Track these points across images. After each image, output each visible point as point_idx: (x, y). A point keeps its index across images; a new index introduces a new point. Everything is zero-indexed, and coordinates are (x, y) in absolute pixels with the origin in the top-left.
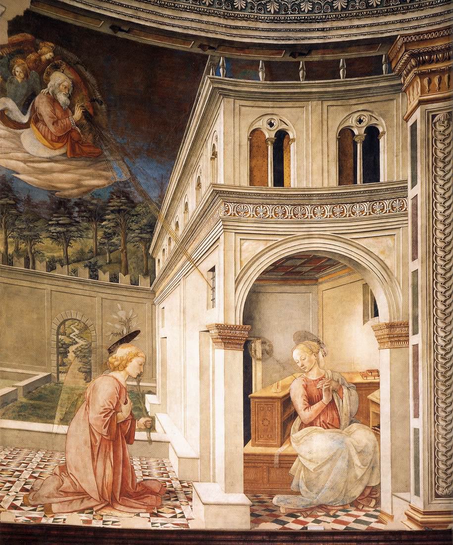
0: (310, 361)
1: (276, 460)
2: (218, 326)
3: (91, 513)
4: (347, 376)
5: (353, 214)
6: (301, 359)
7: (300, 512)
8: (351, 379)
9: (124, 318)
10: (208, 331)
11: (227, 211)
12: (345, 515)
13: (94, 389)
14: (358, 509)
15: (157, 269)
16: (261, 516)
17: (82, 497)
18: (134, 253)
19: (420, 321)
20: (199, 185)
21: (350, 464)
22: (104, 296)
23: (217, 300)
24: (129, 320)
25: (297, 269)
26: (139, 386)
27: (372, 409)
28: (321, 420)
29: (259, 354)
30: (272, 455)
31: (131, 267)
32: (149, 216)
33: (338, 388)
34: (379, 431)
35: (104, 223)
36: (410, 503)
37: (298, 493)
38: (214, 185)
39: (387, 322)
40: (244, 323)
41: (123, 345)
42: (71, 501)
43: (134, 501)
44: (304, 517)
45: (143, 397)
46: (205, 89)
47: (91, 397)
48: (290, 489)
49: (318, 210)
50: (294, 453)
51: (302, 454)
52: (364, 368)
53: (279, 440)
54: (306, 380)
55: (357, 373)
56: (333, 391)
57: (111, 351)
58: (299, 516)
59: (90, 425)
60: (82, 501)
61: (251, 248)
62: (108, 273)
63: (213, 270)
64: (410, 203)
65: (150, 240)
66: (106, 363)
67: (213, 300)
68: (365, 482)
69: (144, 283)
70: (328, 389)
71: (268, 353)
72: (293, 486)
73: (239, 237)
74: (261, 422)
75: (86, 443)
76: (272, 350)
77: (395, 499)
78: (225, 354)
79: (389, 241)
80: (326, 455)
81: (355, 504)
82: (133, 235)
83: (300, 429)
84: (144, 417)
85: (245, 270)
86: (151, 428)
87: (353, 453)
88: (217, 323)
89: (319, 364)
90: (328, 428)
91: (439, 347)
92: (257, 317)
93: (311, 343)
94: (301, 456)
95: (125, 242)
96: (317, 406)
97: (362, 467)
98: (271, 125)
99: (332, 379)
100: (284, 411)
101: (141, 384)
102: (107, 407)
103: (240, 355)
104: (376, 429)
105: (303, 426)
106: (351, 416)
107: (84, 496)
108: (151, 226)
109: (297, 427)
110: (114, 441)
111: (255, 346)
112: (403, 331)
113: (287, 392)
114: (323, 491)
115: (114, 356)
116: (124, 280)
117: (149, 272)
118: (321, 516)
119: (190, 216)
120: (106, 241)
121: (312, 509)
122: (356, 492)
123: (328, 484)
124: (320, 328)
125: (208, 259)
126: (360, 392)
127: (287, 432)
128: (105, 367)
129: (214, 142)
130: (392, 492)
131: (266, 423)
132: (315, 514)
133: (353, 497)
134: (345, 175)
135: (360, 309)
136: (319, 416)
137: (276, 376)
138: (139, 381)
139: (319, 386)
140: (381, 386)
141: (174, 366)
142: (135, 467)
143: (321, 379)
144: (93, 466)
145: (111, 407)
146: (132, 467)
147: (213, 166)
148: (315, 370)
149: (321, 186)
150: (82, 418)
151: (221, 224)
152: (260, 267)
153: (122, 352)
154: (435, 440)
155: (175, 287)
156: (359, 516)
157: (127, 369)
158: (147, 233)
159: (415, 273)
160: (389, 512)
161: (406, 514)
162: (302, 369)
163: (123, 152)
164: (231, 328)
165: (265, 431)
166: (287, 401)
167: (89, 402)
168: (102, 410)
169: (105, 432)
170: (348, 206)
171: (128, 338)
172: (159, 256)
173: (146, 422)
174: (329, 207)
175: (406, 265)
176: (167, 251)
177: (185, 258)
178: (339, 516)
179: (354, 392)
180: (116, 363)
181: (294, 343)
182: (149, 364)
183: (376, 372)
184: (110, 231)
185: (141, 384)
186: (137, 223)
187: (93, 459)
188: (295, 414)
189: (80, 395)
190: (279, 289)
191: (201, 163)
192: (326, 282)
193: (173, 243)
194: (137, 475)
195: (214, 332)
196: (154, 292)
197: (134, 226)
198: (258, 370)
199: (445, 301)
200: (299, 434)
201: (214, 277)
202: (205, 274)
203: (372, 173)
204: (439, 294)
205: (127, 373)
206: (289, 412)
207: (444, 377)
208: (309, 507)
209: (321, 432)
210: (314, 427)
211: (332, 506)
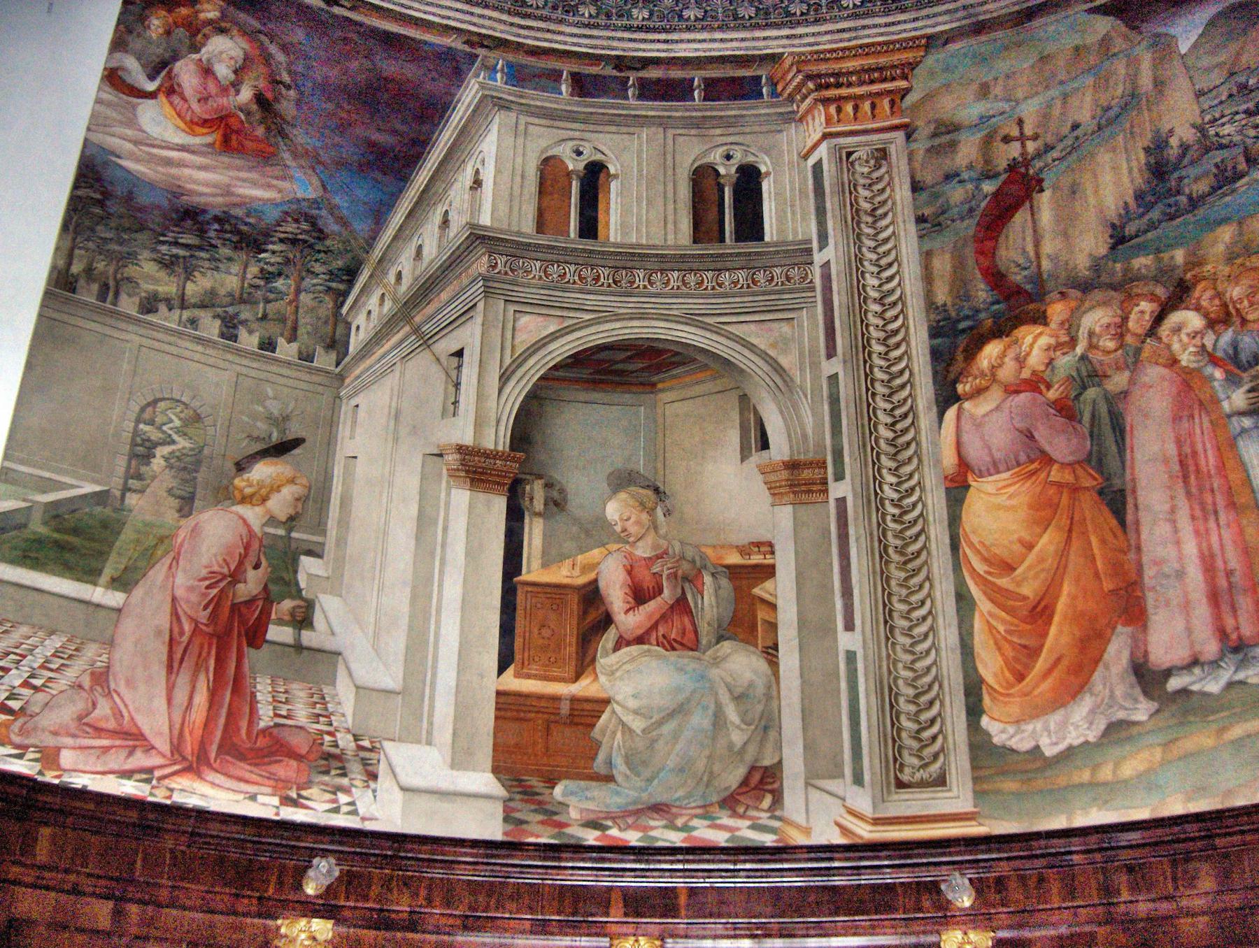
0: (638, 523)
1: (565, 708)
2: (461, 449)
3: (148, 781)
4: (709, 552)
5: (720, 285)
6: (621, 520)
7: (613, 819)
8: (720, 558)
9: (276, 412)
10: (441, 455)
11: (495, 267)
12: (709, 827)
13: (195, 531)
14: (735, 814)
15: (352, 340)
16: (527, 822)
17: (131, 743)
18: (313, 309)
19: (847, 459)
20: (445, 222)
21: (719, 720)
22: (245, 371)
23: (462, 406)
24: (286, 418)
25: (620, 366)
26: (290, 538)
27: (762, 614)
28: (660, 634)
29: (539, 505)
30: (555, 699)
31: (301, 331)
32: (349, 255)
33: (694, 572)
34: (777, 657)
35: (263, 255)
36: (844, 799)
37: (609, 779)
38: (472, 226)
39: (786, 458)
40: (512, 448)
41: (269, 460)
42: (106, 750)
43: (248, 767)
44: (620, 829)
45: (295, 562)
46: (469, 94)
47: (186, 545)
48: (592, 768)
49: (657, 277)
50: (603, 695)
51: (619, 697)
52: (743, 539)
53: (572, 668)
54: (629, 556)
55: (731, 546)
56: (686, 578)
57: (241, 467)
58: (608, 828)
59: (174, 599)
60: (131, 754)
61: (532, 327)
62: (257, 334)
63: (459, 354)
64: (817, 272)
65: (345, 294)
66: (227, 488)
67: (456, 403)
68: (749, 757)
69: (324, 360)
70: (673, 576)
71: (556, 504)
72: (599, 765)
73: (512, 308)
74: (536, 631)
75: (159, 633)
76: (565, 500)
77: (815, 795)
78: (471, 499)
79: (785, 328)
80: (668, 702)
81: (730, 802)
82: (315, 281)
83: (617, 647)
84: (293, 598)
85: (519, 361)
86: (303, 620)
87: (725, 698)
88: (460, 442)
89: (656, 528)
90: (674, 649)
91: (887, 502)
92: (538, 437)
93: (641, 491)
94: (618, 703)
95: (298, 291)
96: (651, 606)
97: (744, 726)
98: (579, 153)
99: (683, 558)
100: (585, 613)
101: (294, 535)
102: (216, 568)
103: (499, 505)
104: (771, 653)
105: (620, 643)
106: (719, 626)
107: (137, 743)
108: (351, 274)
109: (610, 645)
110: (219, 637)
111: (532, 489)
112: (816, 474)
113: (592, 576)
114: (661, 775)
115: (246, 476)
116: (287, 350)
117: (337, 344)
118: (656, 828)
119: (424, 265)
120: (262, 283)
121: (638, 813)
122: (733, 777)
123: (671, 763)
124: (660, 465)
125: (450, 335)
126: (738, 583)
127: (591, 652)
128: (224, 495)
129: (479, 166)
130: (807, 778)
131: (546, 633)
132: (644, 823)
133: (726, 789)
134: (706, 227)
135: (734, 437)
136: (655, 626)
137: (569, 545)
138: (290, 530)
139: (656, 569)
140: (778, 574)
141: (365, 509)
142: (259, 697)
143: (658, 557)
144: (168, 680)
145: (225, 570)
146: (253, 695)
147: (473, 198)
148: (650, 539)
149: (662, 243)
150: (158, 583)
151: (481, 283)
152: (549, 358)
153: (263, 471)
154: (890, 672)
155: (383, 374)
156: (738, 829)
157: (271, 504)
158: (342, 281)
159: (833, 378)
160: (800, 819)
161: (838, 824)
162: (623, 538)
163: (314, 161)
164: (487, 455)
165: (544, 648)
166: (591, 595)
167: (179, 553)
168: (204, 572)
169: (203, 616)
170: (710, 274)
171: (282, 449)
172: (360, 320)
173: (294, 608)
174: (676, 274)
175: (815, 366)
176: (374, 315)
177: (407, 329)
178: (694, 828)
179: (725, 582)
180: (248, 491)
181: (608, 490)
182: (315, 501)
183: (770, 548)
184: (270, 269)
185: (294, 535)
186: (324, 263)
187: (170, 668)
188: (607, 620)
189: (161, 540)
190: (583, 396)
191: (452, 193)
192: (671, 389)
193: (388, 304)
194: (261, 712)
195: (452, 458)
196: (341, 378)
197: (318, 268)
198: (534, 534)
199: (893, 424)
200: (613, 658)
201: (459, 367)
202: (444, 360)
203: (750, 226)
204: (879, 413)
205: (268, 511)
206: (593, 616)
207: (902, 554)
208: (630, 808)
209: (659, 657)
210: (646, 647)
211: (680, 807)
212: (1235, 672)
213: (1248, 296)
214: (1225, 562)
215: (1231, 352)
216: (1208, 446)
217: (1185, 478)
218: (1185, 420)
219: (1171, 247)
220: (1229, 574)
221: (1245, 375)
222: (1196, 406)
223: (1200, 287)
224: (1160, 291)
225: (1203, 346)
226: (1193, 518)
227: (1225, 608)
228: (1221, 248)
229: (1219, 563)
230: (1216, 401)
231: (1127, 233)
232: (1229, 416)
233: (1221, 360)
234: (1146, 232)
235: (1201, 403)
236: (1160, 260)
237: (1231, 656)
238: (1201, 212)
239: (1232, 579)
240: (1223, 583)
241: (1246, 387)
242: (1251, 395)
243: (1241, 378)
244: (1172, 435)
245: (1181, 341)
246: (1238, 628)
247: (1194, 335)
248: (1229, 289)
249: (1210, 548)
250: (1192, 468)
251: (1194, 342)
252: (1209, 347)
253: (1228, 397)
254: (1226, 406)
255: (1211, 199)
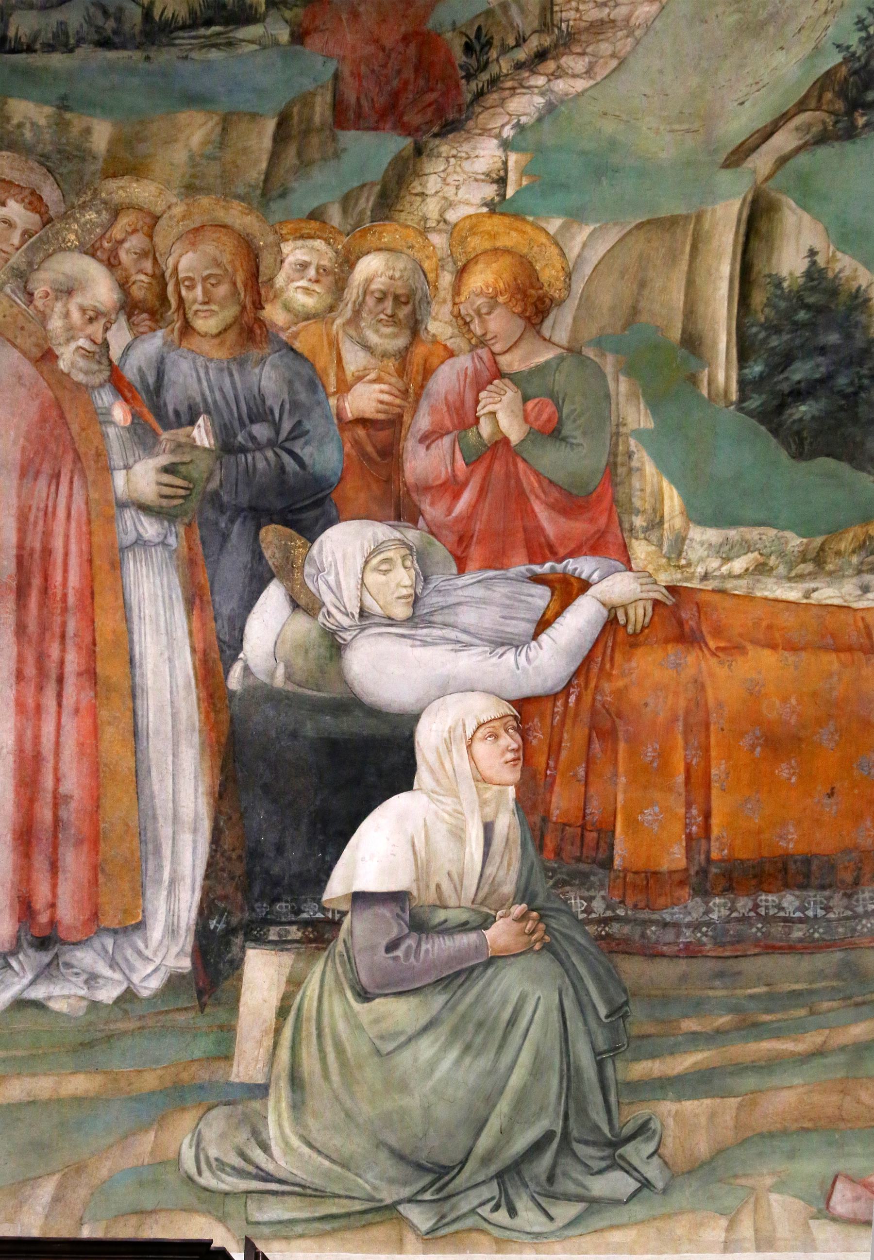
212: (33, 983)
213: (205, 279)
214: (57, 780)
215: (151, 380)
216: (73, 548)
217: (21, 593)
218: (42, 482)
219: (90, 106)
220: (58, 800)
221: (165, 435)
222: (70, 457)
223: (125, 221)
224: (50, 193)
225: (106, 345)
226: (20, 676)
227: (40, 862)
228: (179, 155)
229: (48, 782)
230: (108, 470)
231: (11, 33)
232: (122, 505)
233: (130, 386)
234: (49, 48)
235: (77, 458)
236: (61, 125)
237: (31, 952)
238: (164, 57)
239: (63, 814)
240: (45, 814)
241: (164, 460)
242: (167, 478)
243: (156, 435)
244: (14, 501)
245: (67, 315)
246: (53, 906)
247: (93, 316)
248: (177, 249)
249: (37, 738)
250: (36, 581)
251: (90, 329)
252: (115, 353)
253: (127, 467)
254: (120, 479)
255: (184, 39)
